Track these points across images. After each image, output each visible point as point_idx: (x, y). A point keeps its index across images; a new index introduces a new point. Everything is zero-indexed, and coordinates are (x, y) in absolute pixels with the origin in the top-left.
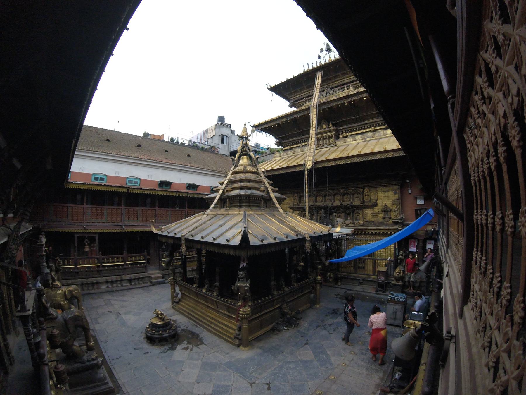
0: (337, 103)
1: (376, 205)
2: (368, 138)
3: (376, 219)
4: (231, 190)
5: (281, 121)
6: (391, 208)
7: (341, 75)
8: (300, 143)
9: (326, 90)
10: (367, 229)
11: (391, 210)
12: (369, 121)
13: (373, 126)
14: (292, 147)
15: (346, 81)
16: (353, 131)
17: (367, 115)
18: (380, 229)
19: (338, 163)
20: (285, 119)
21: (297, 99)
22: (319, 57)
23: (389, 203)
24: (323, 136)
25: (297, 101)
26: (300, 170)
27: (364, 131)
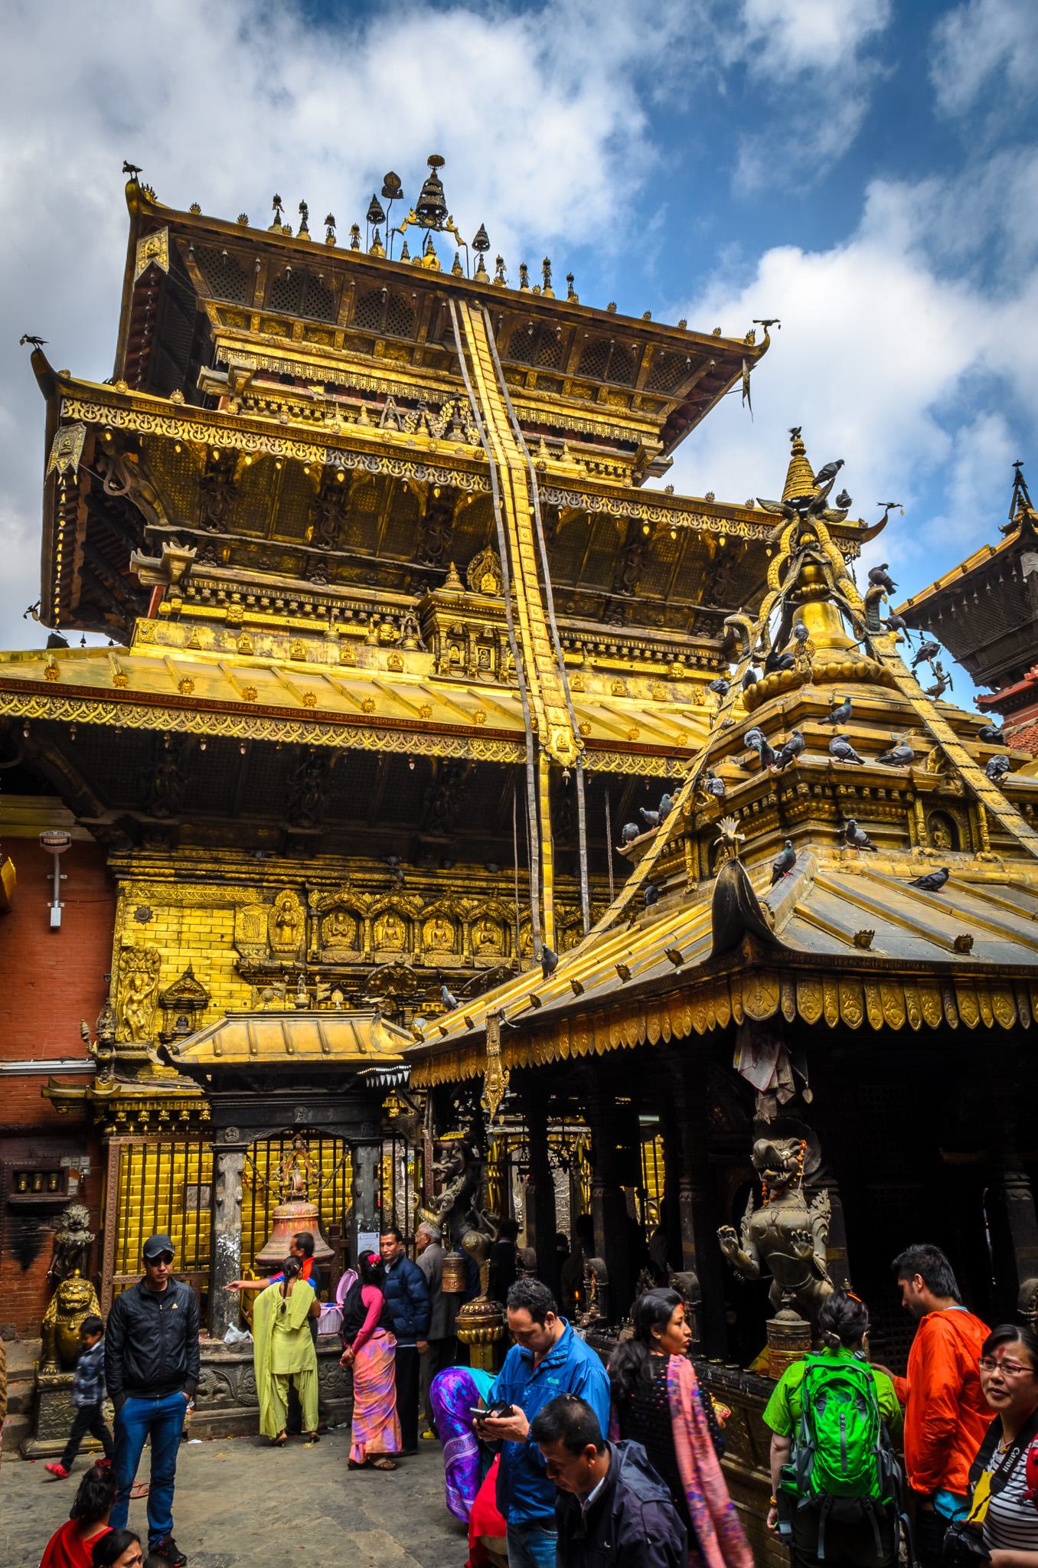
2: (676, 699)
7: (532, 379)
9: (448, 410)
13: (676, 659)
14: (249, 616)
15: (543, 417)
17: (663, 609)
21: (265, 363)
24: (479, 629)
26: (488, 756)
27: (638, 666)
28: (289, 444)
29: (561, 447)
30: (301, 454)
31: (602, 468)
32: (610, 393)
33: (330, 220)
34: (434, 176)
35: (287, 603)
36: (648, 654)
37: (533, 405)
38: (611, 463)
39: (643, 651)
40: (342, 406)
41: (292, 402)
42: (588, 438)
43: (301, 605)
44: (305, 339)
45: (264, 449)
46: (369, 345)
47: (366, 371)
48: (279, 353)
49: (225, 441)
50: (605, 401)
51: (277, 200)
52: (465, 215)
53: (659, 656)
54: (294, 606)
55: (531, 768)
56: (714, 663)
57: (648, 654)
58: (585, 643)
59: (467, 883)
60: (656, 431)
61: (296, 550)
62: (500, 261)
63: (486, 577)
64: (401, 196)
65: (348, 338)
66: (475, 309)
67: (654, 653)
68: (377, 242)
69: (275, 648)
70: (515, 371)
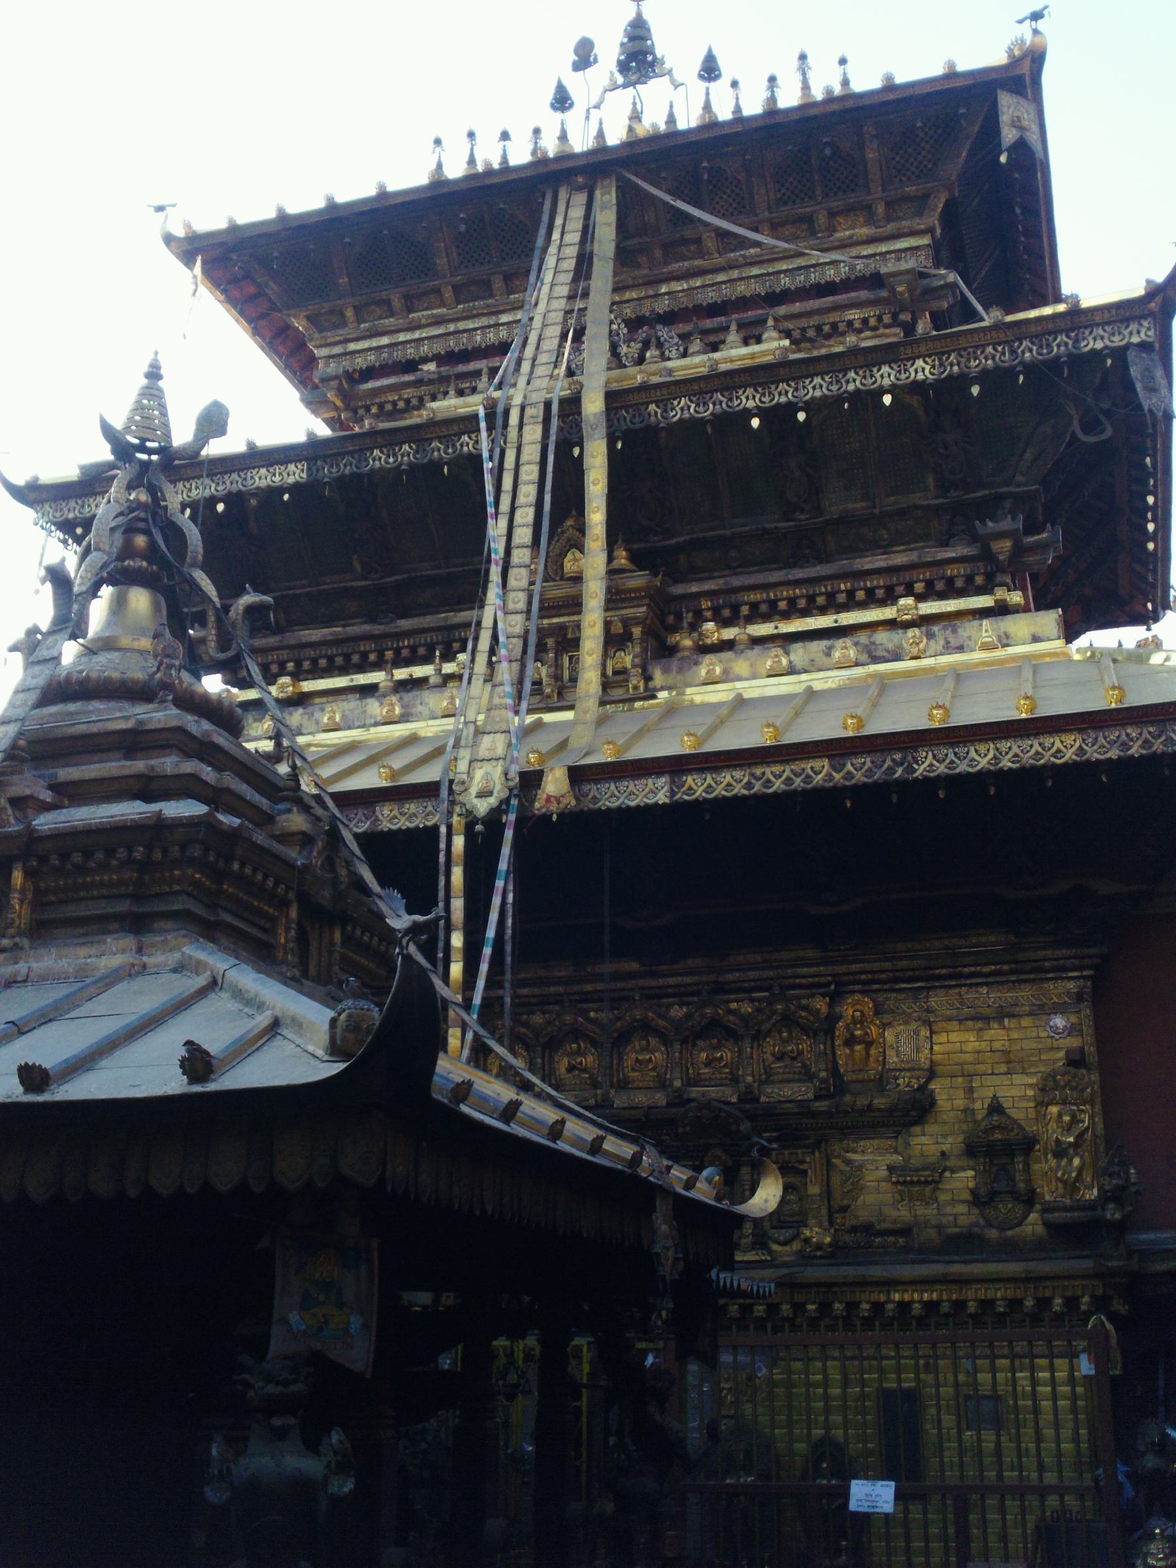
0: (683, 409)
1: (919, 1108)
3: (922, 1211)
4: (47, 796)
5: (262, 478)
6: (1031, 1128)
8: (377, 666)
10: (865, 1283)
11: (1028, 1145)
12: (880, 561)
13: (909, 592)
14: (308, 686)
15: (742, 289)
16: (766, 618)
18: (964, 1282)
19: (698, 786)
20: (295, 474)
21: (372, 357)
22: (562, 101)
23: (1017, 1093)
25: (369, 373)
26: (404, 823)
28: (263, 471)
29: (765, 321)
30: (277, 479)
31: (842, 327)
32: (832, 215)
33: (505, 136)
34: (639, 15)
35: (347, 658)
36: (860, 595)
37: (721, 277)
38: (854, 315)
39: (851, 594)
40: (462, 376)
41: (408, 393)
42: (828, 289)
43: (364, 655)
44: (410, 311)
45: (234, 488)
46: (486, 289)
47: (492, 320)
48: (385, 340)
49: (194, 493)
50: (832, 229)
51: (438, 142)
52: (675, 47)
53: (880, 593)
54: (356, 658)
55: (443, 829)
56: (979, 580)
57: (860, 595)
58: (754, 606)
59: (536, 991)
60: (925, 240)
61: (346, 588)
62: (734, 84)
63: (569, 556)
64: (596, 61)
65: (455, 288)
66: (579, 189)
67: (870, 592)
68: (563, 137)
69: (305, 722)
70: (685, 242)
